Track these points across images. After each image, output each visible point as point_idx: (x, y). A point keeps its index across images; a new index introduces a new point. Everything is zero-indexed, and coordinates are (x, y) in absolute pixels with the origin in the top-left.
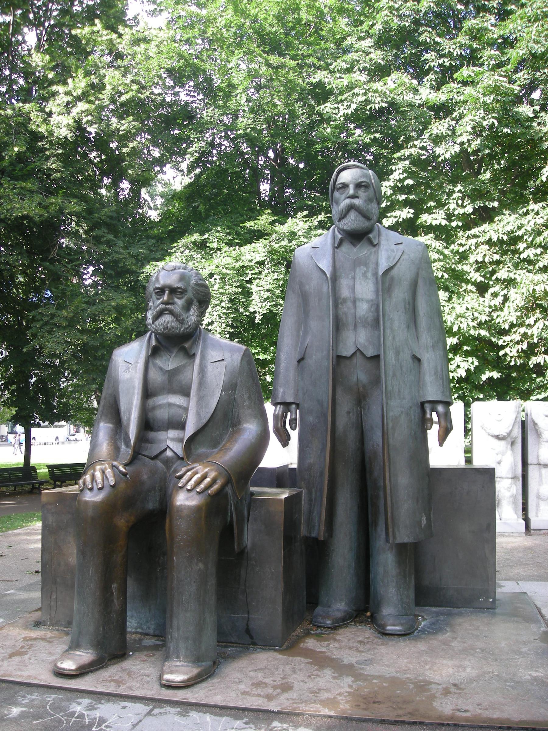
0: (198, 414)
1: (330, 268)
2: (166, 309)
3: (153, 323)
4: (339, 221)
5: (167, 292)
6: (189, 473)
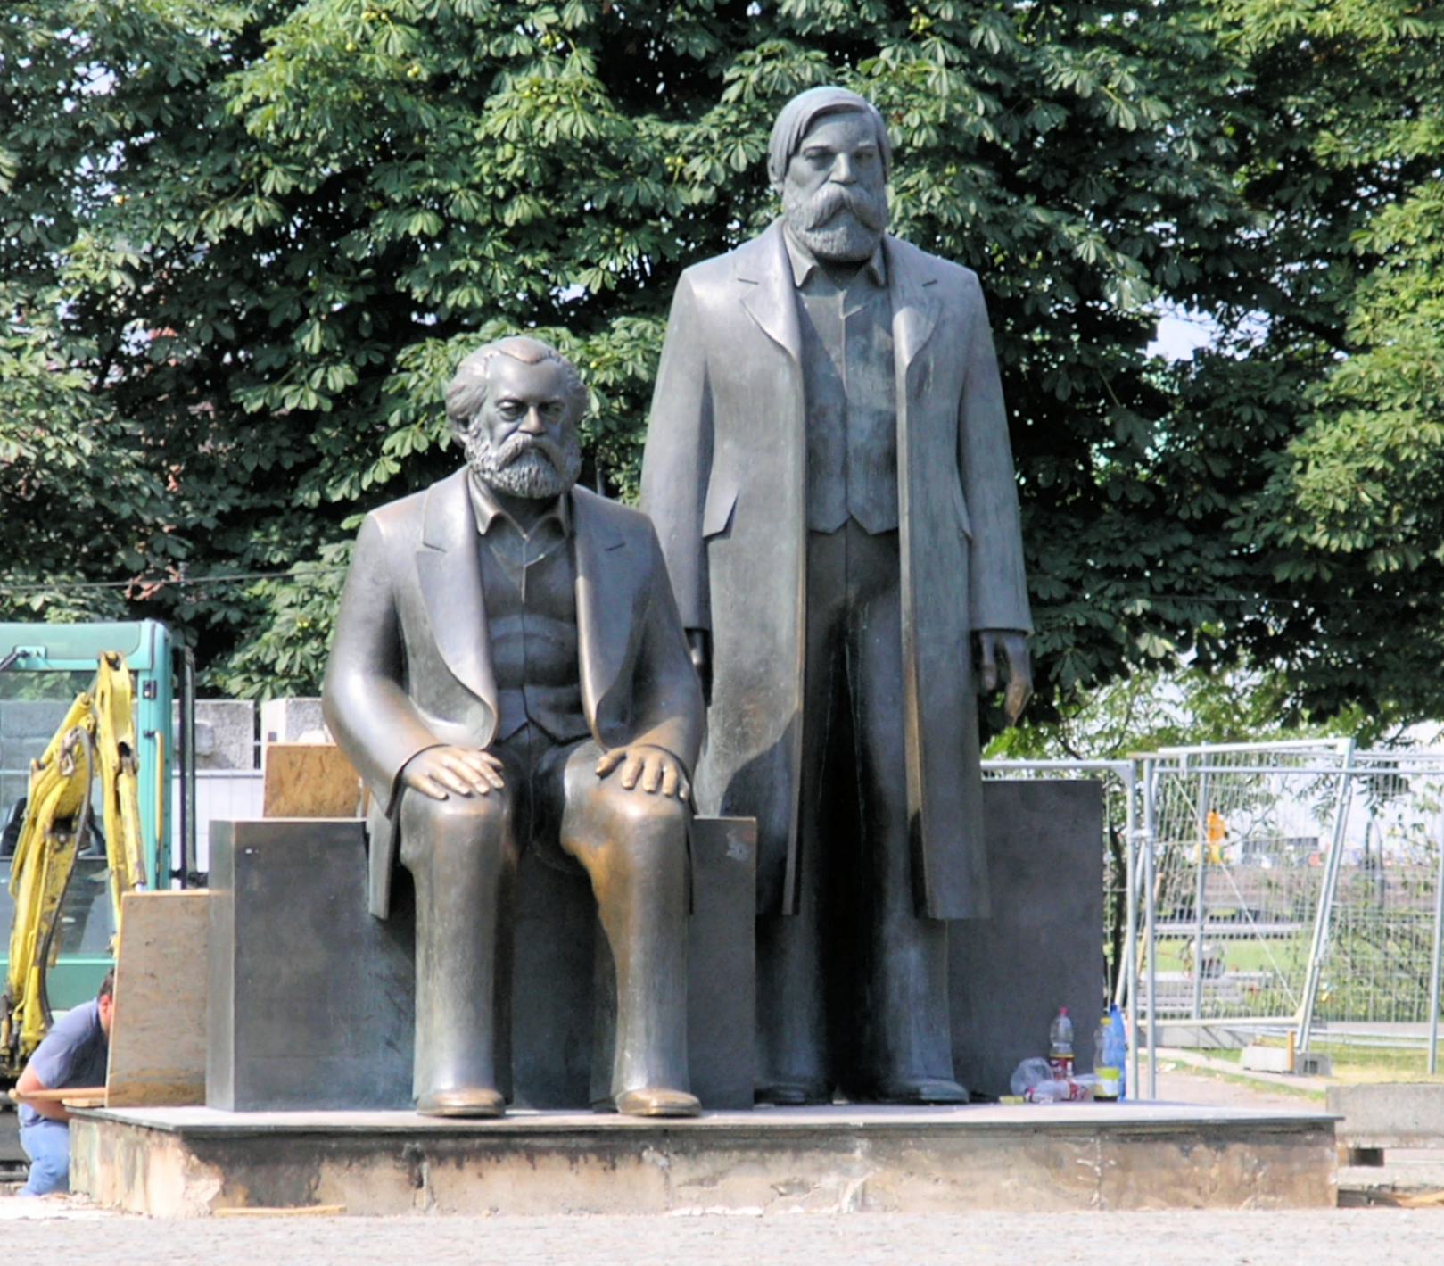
4: (813, 229)
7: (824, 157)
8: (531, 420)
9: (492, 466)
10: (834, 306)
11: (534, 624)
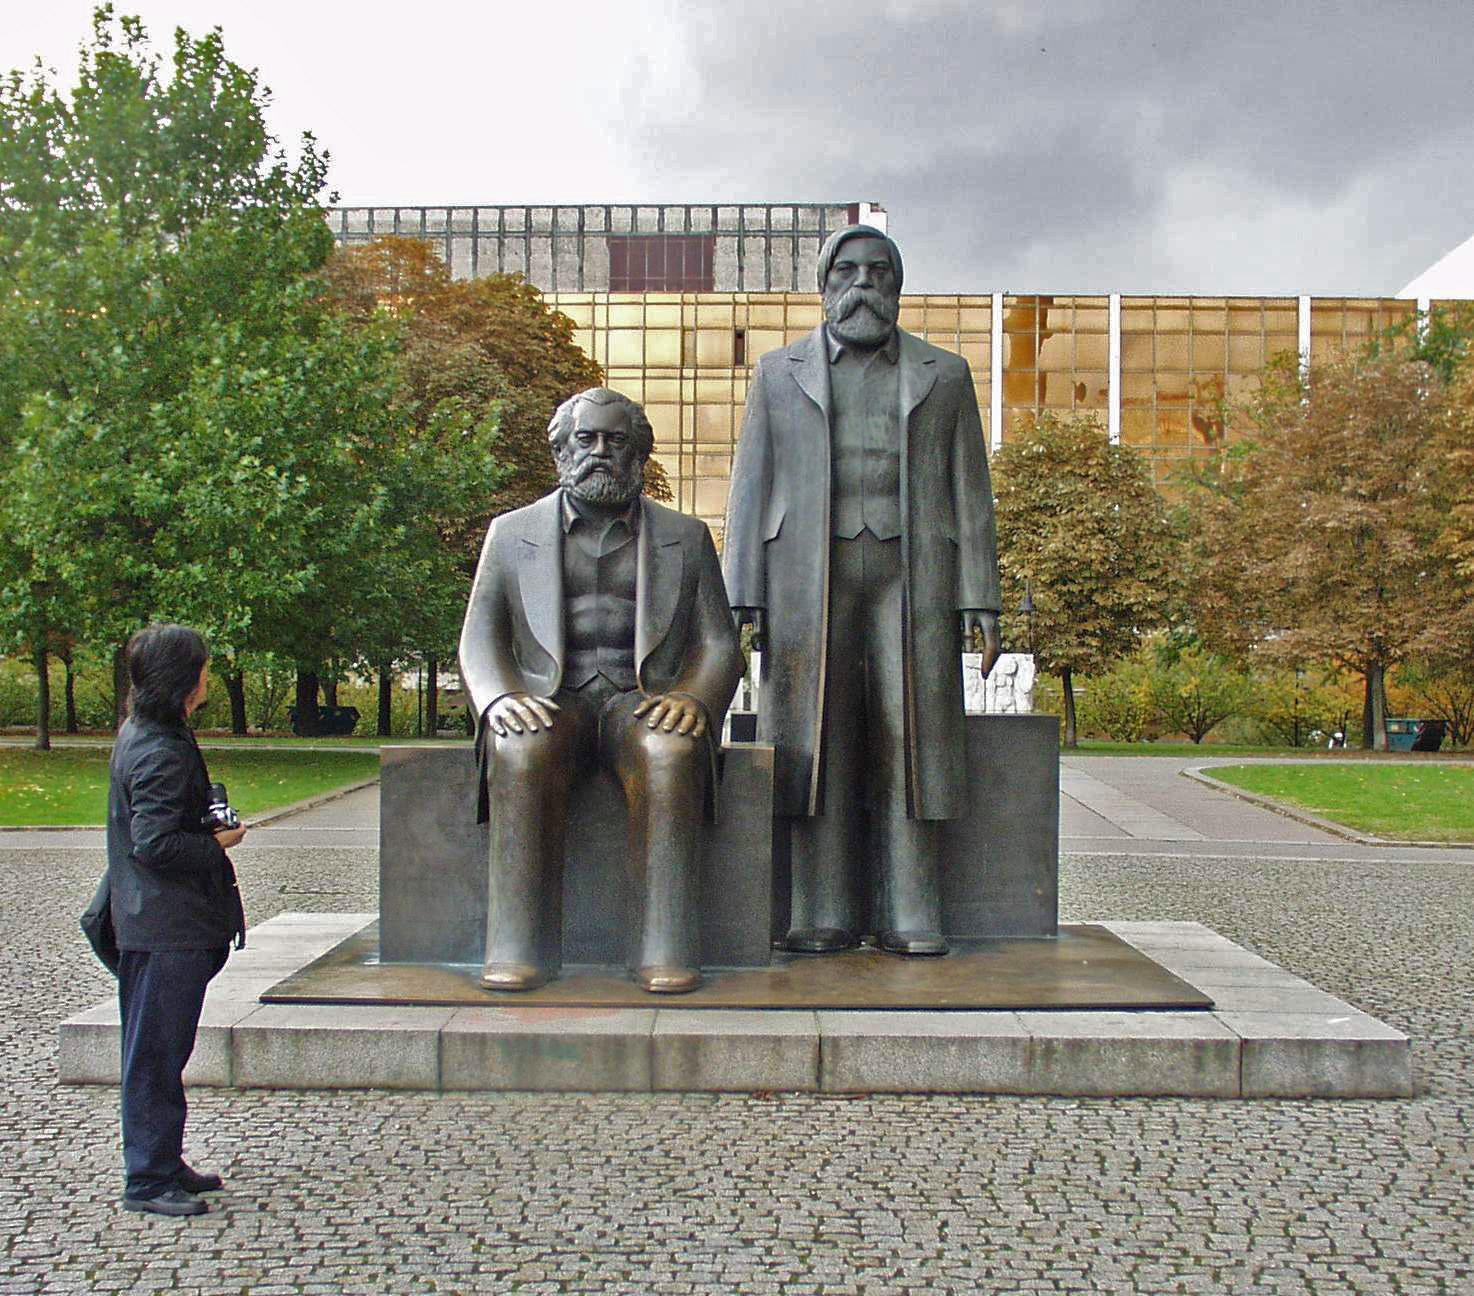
0: (653, 624)
1: (827, 401)
2: (600, 465)
3: (577, 483)
4: (841, 321)
5: (600, 439)
6: (658, 710)
7: (851, 267)
8: (599, 448)
9: (572, 482)
10: (854, 375)
11: (608, 600)
